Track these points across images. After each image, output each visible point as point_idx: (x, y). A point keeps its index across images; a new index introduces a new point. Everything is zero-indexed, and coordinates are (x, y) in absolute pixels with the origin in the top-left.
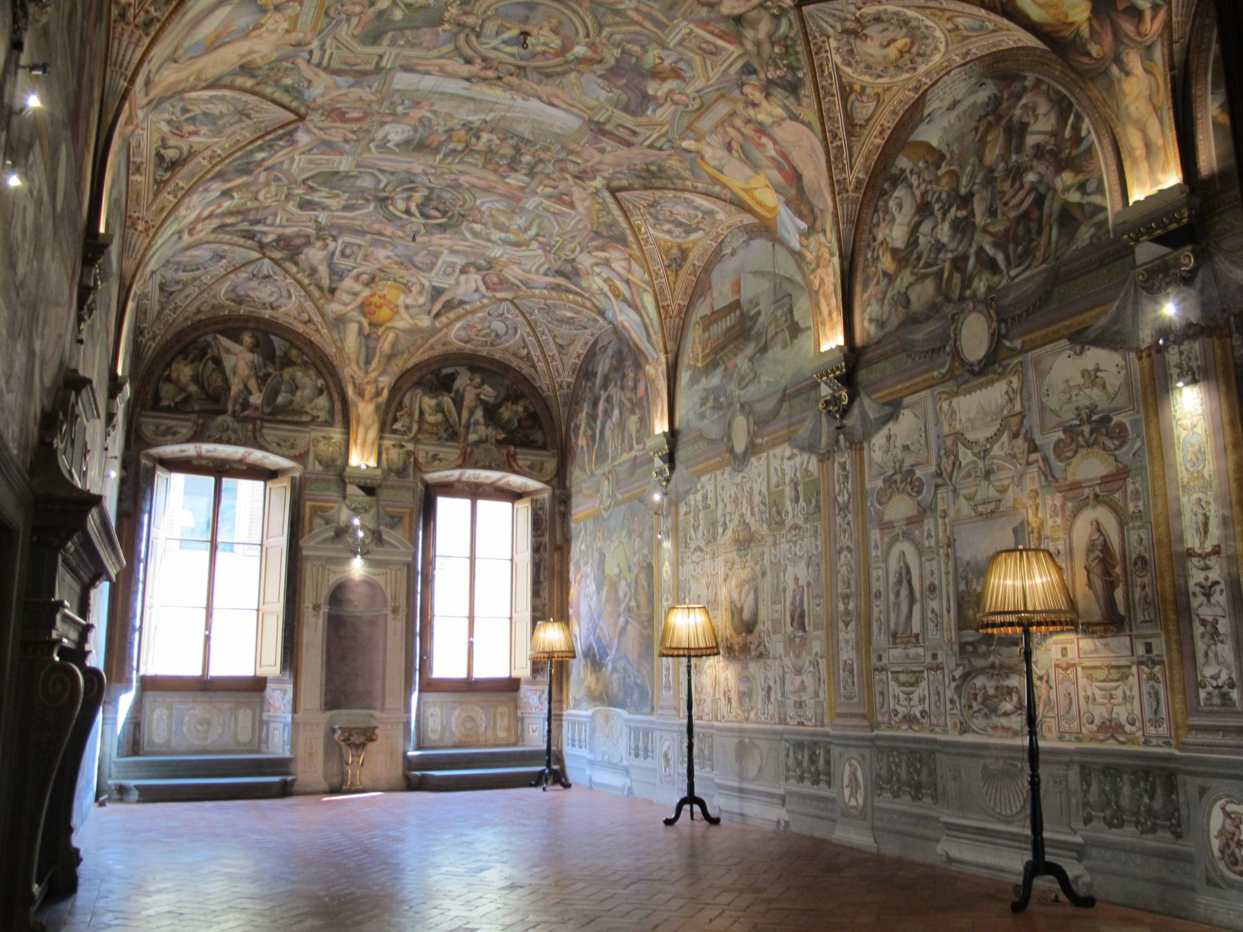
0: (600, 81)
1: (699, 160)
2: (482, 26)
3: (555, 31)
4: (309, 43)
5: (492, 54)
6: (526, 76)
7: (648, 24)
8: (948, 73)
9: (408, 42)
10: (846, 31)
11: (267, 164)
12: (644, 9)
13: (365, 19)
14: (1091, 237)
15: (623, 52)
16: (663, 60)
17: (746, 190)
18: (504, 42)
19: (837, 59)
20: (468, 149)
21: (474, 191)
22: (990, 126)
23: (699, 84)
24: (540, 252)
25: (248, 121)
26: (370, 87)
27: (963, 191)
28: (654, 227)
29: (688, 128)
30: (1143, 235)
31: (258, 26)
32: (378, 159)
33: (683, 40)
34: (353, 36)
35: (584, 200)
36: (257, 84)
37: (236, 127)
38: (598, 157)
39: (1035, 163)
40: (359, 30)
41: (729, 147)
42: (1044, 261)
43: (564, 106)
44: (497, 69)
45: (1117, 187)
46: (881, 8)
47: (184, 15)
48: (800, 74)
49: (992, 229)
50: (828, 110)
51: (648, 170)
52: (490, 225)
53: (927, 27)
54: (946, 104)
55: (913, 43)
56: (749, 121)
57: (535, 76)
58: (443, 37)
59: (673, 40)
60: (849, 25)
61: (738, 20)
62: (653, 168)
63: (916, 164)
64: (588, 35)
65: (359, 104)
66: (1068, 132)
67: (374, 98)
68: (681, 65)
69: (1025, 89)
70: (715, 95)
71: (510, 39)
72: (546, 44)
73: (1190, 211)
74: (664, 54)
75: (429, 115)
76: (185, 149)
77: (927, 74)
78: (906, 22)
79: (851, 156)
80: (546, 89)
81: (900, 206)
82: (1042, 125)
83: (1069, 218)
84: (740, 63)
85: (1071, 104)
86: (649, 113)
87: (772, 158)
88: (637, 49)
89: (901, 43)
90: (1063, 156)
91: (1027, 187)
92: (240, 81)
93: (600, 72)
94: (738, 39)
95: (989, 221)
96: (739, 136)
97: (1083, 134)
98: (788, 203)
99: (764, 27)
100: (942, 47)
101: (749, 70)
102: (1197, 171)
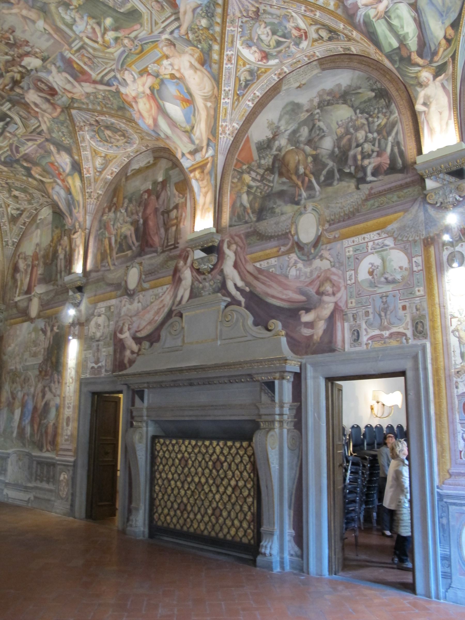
13: (127, 31)
25: (262, 7)
31: (173, 76)
34: (142, 25)
36: (216, 40)
47: (168, 137)
76: (314, 28)
92: (215, 57)
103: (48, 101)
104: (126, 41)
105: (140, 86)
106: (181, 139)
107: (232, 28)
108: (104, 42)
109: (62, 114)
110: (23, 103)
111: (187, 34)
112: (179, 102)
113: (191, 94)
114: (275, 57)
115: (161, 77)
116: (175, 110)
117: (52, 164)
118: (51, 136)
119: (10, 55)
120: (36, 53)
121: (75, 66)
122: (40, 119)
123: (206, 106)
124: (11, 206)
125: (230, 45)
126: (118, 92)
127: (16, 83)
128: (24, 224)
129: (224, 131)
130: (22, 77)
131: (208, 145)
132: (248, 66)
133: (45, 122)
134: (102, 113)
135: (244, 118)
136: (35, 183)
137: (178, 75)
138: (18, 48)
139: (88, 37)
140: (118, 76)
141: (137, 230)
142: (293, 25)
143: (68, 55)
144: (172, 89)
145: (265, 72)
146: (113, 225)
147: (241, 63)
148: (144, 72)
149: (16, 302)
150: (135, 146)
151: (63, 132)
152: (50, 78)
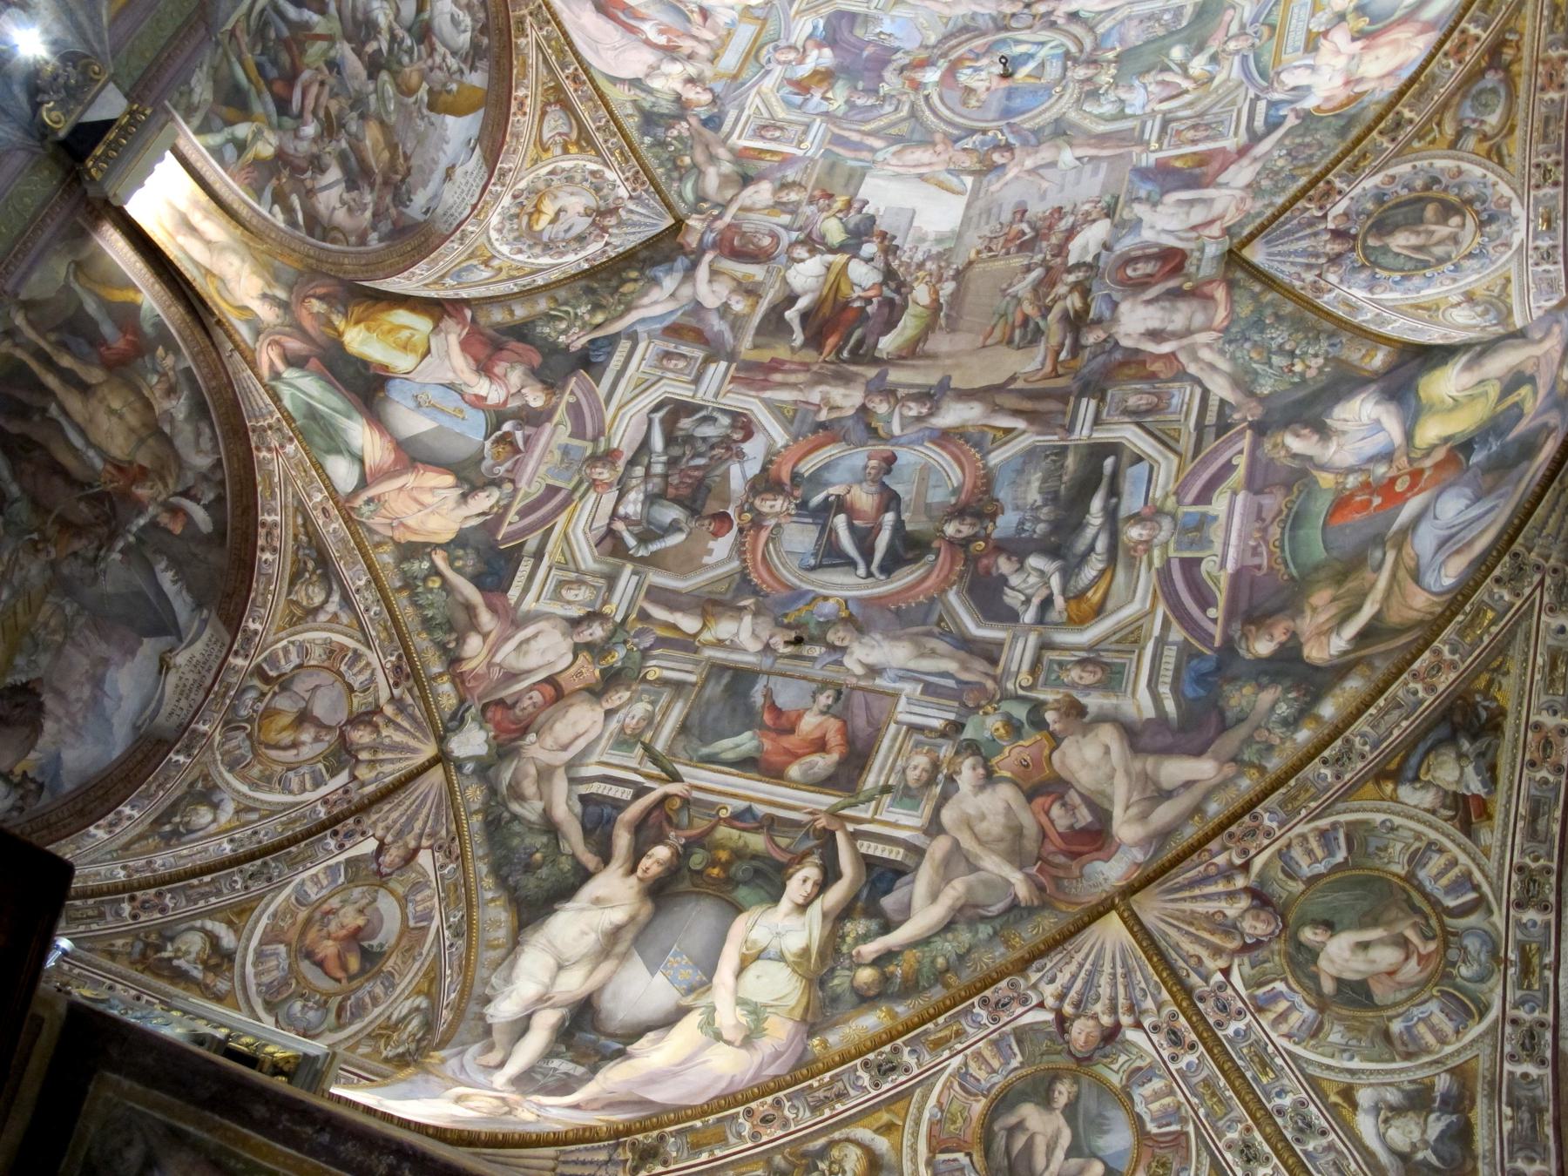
0: (897, 44)
2: (1065, 69)
3: (969, 91)
5: (1043, 35)
6: (994, 19)
7: (855, 137)
8: (474, 207)
10: (613, 211)
12: (865, 155)
13: (1220, 35)
14: (191, 91)
16: (824, 98)
18: (1031, 56)
19: (610, 175)
22: (392, 166)
23: (768, 84)
27: (384, 76)
29: (765, 20)
30: (129, 124)
33: (805, 133)
39: (315, 149)
40: (1227, 18)
41: (705, 13)
42: (232, 34)
45: (199, 165)
46: (583, 254)
48: (648, 140)
49: (320, 45)
50: (596, 108)
53: (520, 251)
54: (459, 171)
55: (530, 226)
56: (690, 57)
57: (981, 22)
58: (1113, 40)
59: (818, 127)
60: (612, 221)
61: (746, 180)
63: (460, 83)
64: (927, 98)
66: (295, 201)
68: (798, 99)
69: (374, 228)
70: (744, 75)
71: (1025, 63)
72: (977, 70)
73: (93, 179)
74: (825, 106)
77: (497, 197)
78: (547, 247)
79: (545, 60)
81: (455, 22)
82: (331, 195)
83: (234, 102)
84: (726, 128)
85: (311, 233)
86: (821, 23)
87: (643, 19)
88: (859, 102)
89: (544, 221)
90: (286, 172)
91: (308, 116)
95: (332, 53)
96: (695, 31)
97: (277, 208)
99: (711, 182)
100: (494, 235)
101: (713, 122)
102: (117, 225)
103: (1176, 294)
108: (1195, 80)
109: (1238, 293)
110: (1123, 364)
117: (1342, 503)
118: (1262, 400)
119: (1037, 265)
120: (1088, 213)
121: (1178, 164)
122: (1192, 369)
124: (1364, 1097)
126: (1307, 117)
127: (1076, 322)
130: (1085, 293)
133: (1212, 367)
136: (1354, 685)
138: (1046, 237)
140: (1276, 96)
143: (1148, 160)
150: (1517, 209)
151: (1281, 350)
152: (1147, 235)
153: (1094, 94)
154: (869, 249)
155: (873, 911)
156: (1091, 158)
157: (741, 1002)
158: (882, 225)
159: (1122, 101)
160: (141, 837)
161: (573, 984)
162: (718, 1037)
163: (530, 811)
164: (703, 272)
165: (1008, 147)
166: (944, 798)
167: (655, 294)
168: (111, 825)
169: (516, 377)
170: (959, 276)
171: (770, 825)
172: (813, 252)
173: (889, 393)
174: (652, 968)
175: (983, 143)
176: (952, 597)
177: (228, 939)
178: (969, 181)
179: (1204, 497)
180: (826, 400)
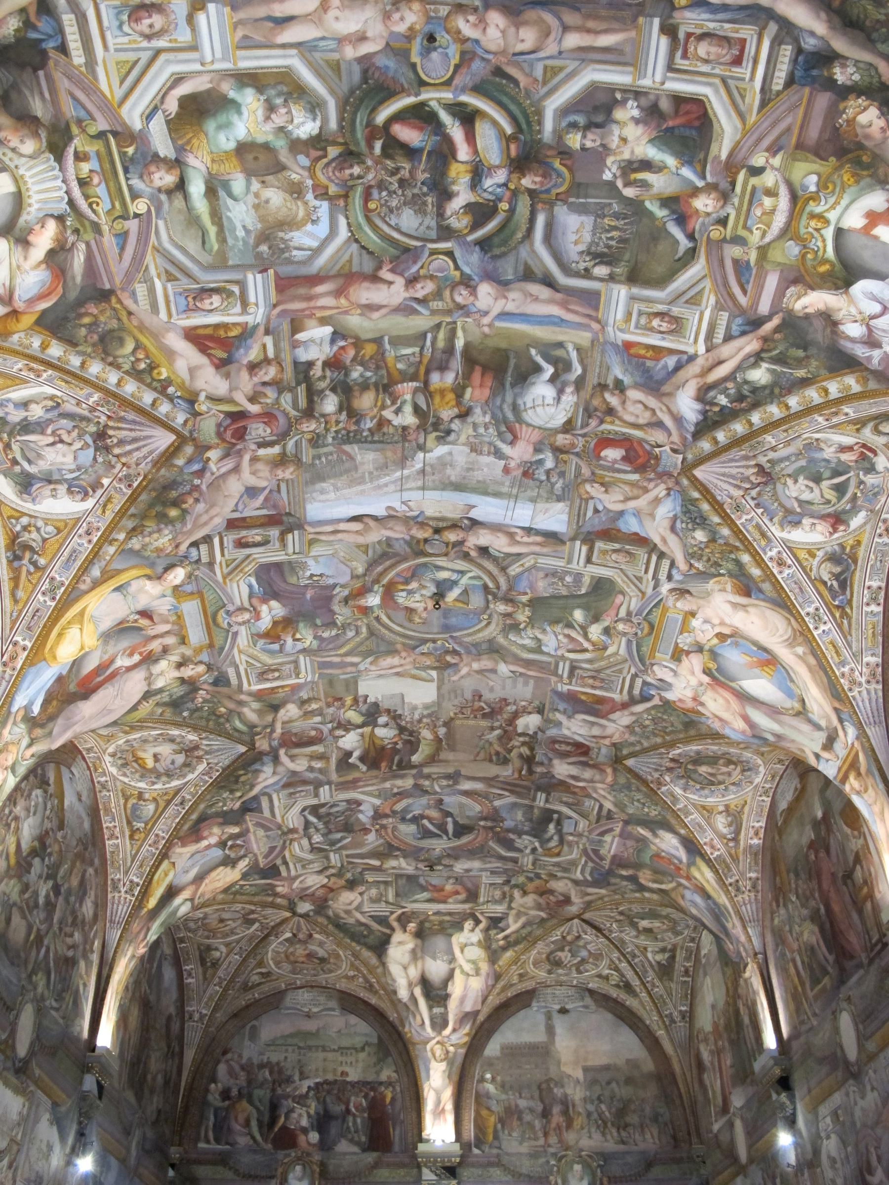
0: (331, 581)
1: (148, 571)
2: (488, 602)
3: (410, 611)
4: (671, 591)
5: (461, 565)
6: (408, 543)
7: (337, 660)
9: (562, 579)
11: (750, 345)
12: (349, 669)
13: (612, 612)
15: (332, 624)
17: (82, 613)
20: (419, 374)
21: (368, 266)
23: (243, 640)
24: (133, 115)
25: (762, 460)
26: (596, 511)
28: (52, 398)
31: (722, 637)
32: (561, 322)
34: (622, 593)
35: (192, 371)
37: (783, 453)
38: (248, 478)
41: (145, 614)
43: (342, 526)
44: (447, 544)
47: (779, 737)
51: (175, 504)
52: (280, 144)
56: (165, 650)
58: (523, 585)
61: (275, 708)
62: (173, 513)
64: (377, 619)
65: (609, 476)
67: (588, 487)
68: (276, 647)
70: (218, 642)
71: (451, 589)
72: (410, 592)
74: (300, 646)
75: (506, 449)
80: (376, 535)
86: (253, 581)
87: (112, 662)
88: (326, 635)
92: (756, 572)
93: (338, 589)
94: (258, 696)
96: (151, 633)
98: (60, 679)
101: (221, 681)
103: (585, 764)
104: (621, 627)
105: (690, 677)
106: (799, 731)
107: (745, 517)
108: (594, 644)
111: (691, 565)
112: (757, 671)
113: (765, 650)
114: (855, 509)
115: (707, 647)
116: (760, 686)
121: (583, 697)
123: (799, 657)
125: (763, 543)
128: (686, 972)
129: (853, 682)
131: (841, 721)
132: (820, 554)
134: (672, 745)
135: (880, 639)
136: (655, 897)
137: (727, 631)
139: (569, 651)
140: (649, 680)
141: (822, 930)
142: (832, 449)
143: (564, 688)
144: (734, 658)
145: (859, 543)
146: (791, 931)
147: (802, 555)
148: (678, 655)
149: (716, 1136)
150: (762, 769)
152: (566, 732)
153: (515, 627)
154: (382, 720)
155: (496, 927)
156: (521, 674)
157: (469, 961)
158: (385, 705)
159: (539, 640)
160: (204, 973)
161: (414, 973)
162: (468, 975)
163: (351, 921)
164: (284, 758)
165: (455, 652)
166: (511, 901)
167: (262, 776)
168: (190, 975)
169: (216, 830)
170: (446, 724)
171: (450, 914)
172: (347, 730)
173: (428, 777)
174: (434, 958)
175: (436, 649)
176: (491, 843)
177: (264, 970)
178: (434, 673)
179: (602, 834)
180: (394, 786)
